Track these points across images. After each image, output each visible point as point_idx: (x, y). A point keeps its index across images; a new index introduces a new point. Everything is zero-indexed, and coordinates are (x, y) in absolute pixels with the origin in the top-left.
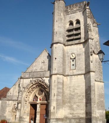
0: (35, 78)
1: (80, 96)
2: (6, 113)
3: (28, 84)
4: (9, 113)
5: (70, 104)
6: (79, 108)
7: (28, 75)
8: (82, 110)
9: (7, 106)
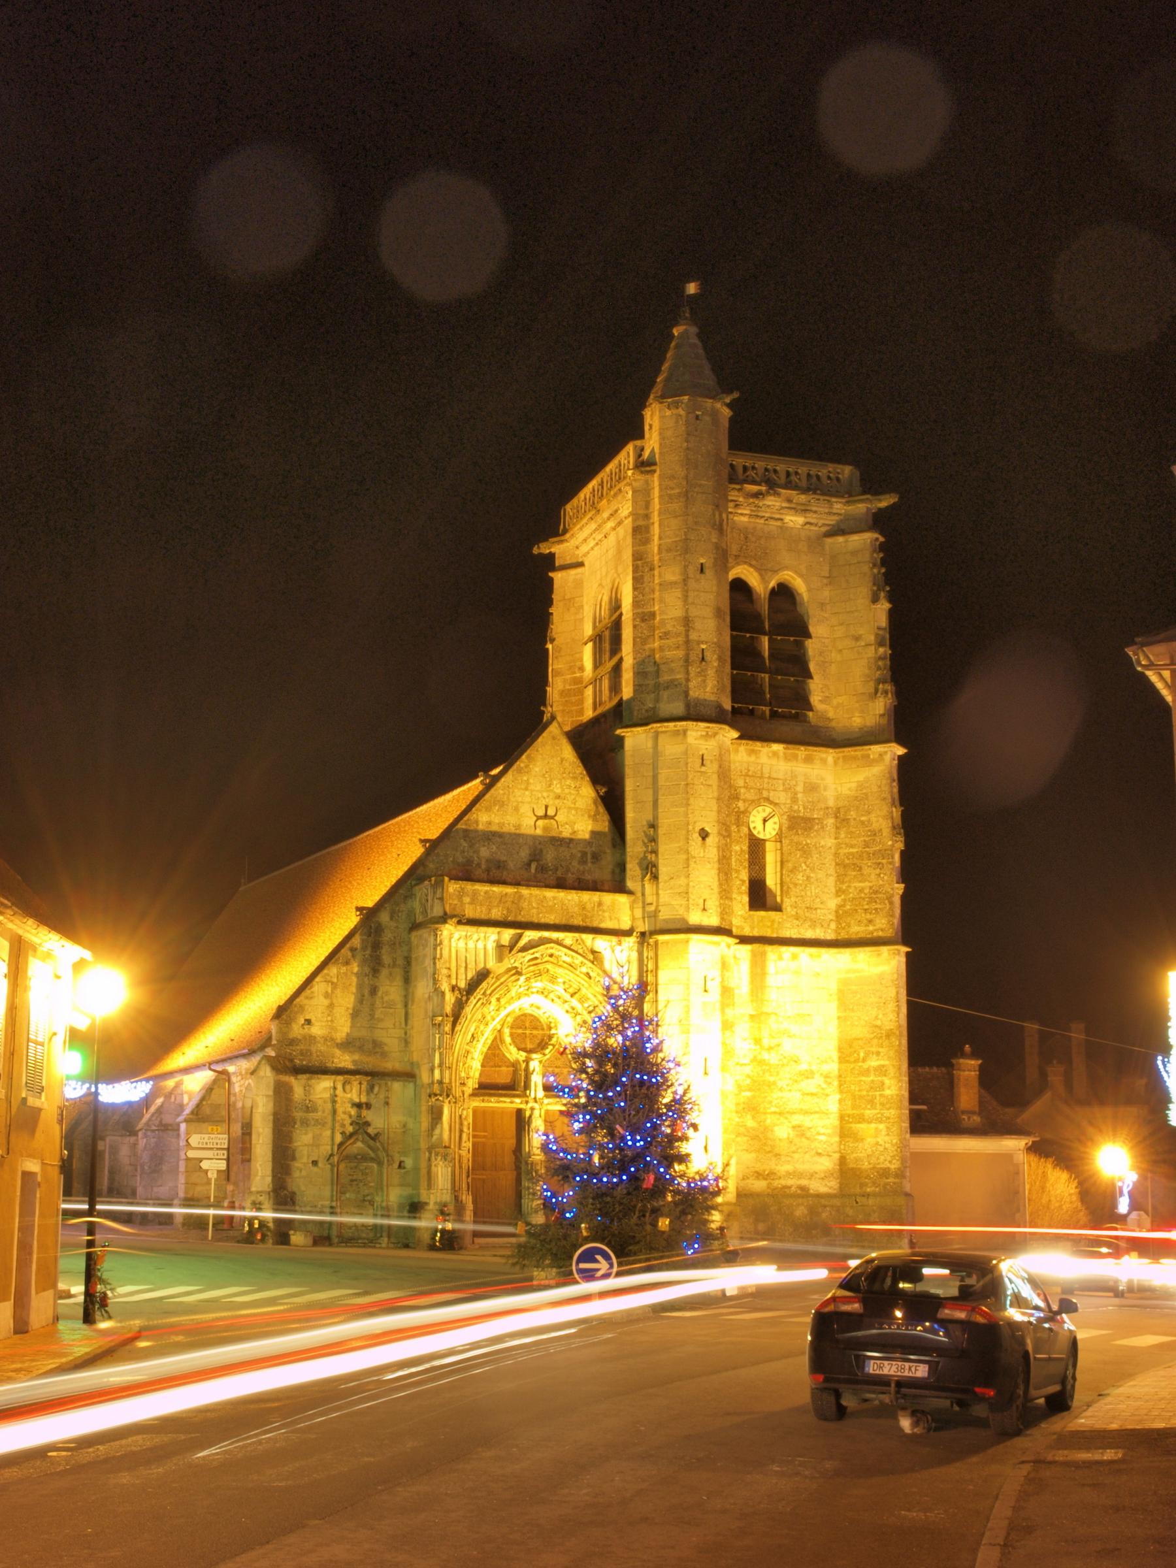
1: (809, 1075)
2: (296, 1174)
4: (315, 1169)
5: (753, 1118)
6: (805, 1142)
8: (820, 1154)
9: (298, 1115)
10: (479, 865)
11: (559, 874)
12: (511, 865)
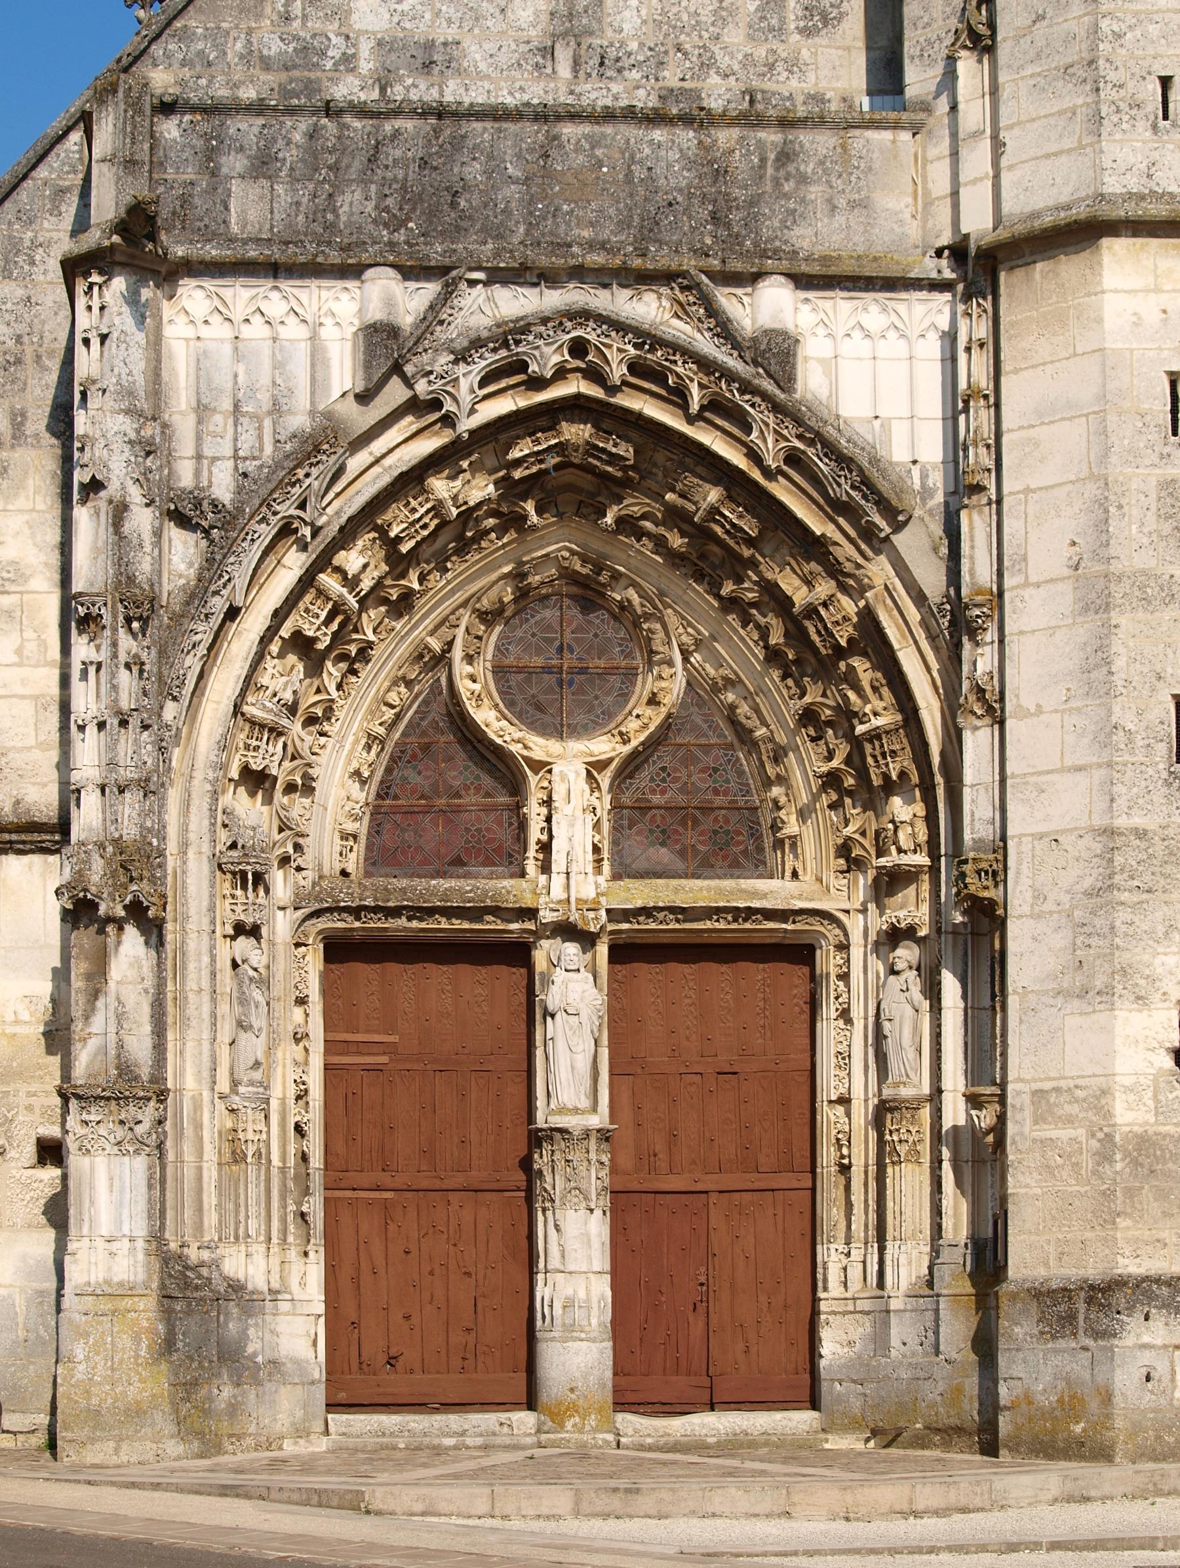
0: (498, 277)
3: (299, 421)
7: (263, 166)
10: (348, 62)
11: (671, 78)
12: (475, 54)
